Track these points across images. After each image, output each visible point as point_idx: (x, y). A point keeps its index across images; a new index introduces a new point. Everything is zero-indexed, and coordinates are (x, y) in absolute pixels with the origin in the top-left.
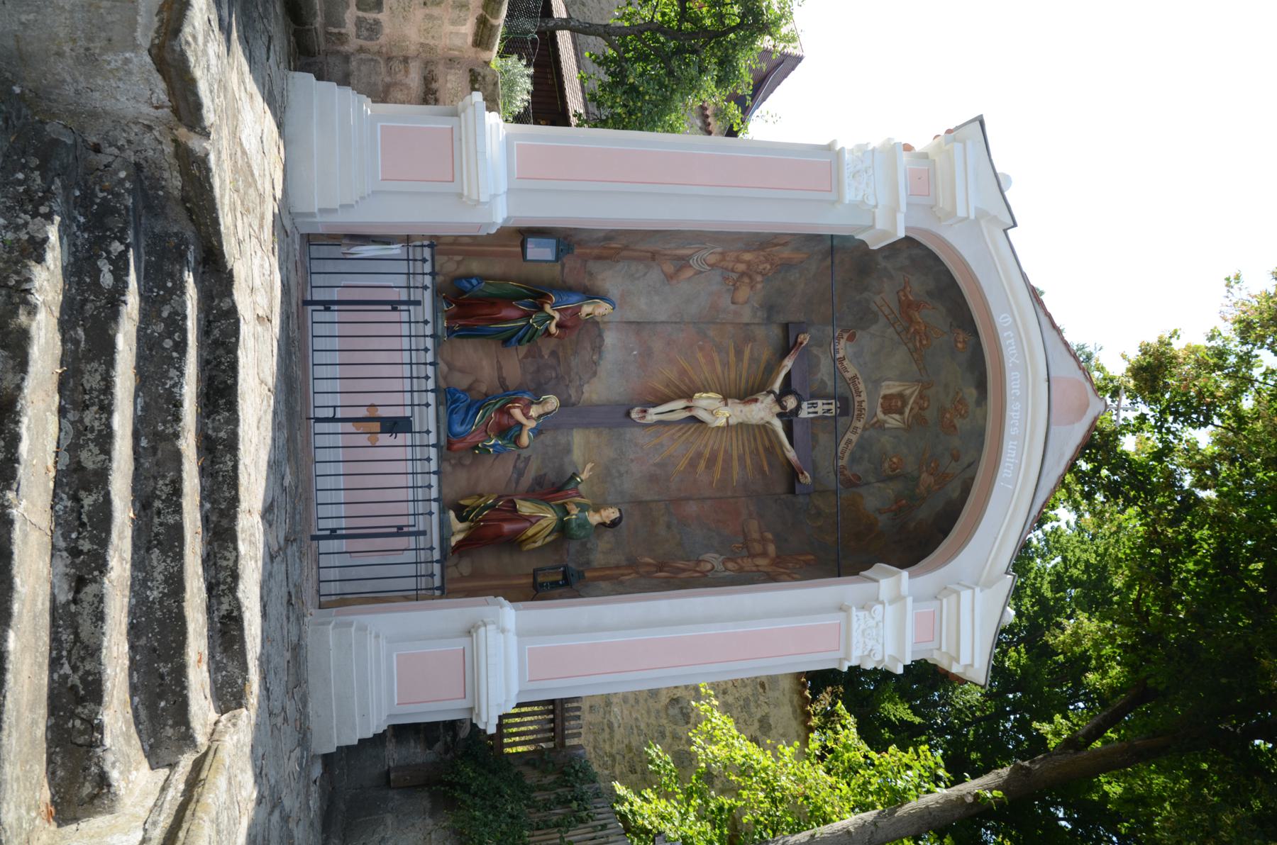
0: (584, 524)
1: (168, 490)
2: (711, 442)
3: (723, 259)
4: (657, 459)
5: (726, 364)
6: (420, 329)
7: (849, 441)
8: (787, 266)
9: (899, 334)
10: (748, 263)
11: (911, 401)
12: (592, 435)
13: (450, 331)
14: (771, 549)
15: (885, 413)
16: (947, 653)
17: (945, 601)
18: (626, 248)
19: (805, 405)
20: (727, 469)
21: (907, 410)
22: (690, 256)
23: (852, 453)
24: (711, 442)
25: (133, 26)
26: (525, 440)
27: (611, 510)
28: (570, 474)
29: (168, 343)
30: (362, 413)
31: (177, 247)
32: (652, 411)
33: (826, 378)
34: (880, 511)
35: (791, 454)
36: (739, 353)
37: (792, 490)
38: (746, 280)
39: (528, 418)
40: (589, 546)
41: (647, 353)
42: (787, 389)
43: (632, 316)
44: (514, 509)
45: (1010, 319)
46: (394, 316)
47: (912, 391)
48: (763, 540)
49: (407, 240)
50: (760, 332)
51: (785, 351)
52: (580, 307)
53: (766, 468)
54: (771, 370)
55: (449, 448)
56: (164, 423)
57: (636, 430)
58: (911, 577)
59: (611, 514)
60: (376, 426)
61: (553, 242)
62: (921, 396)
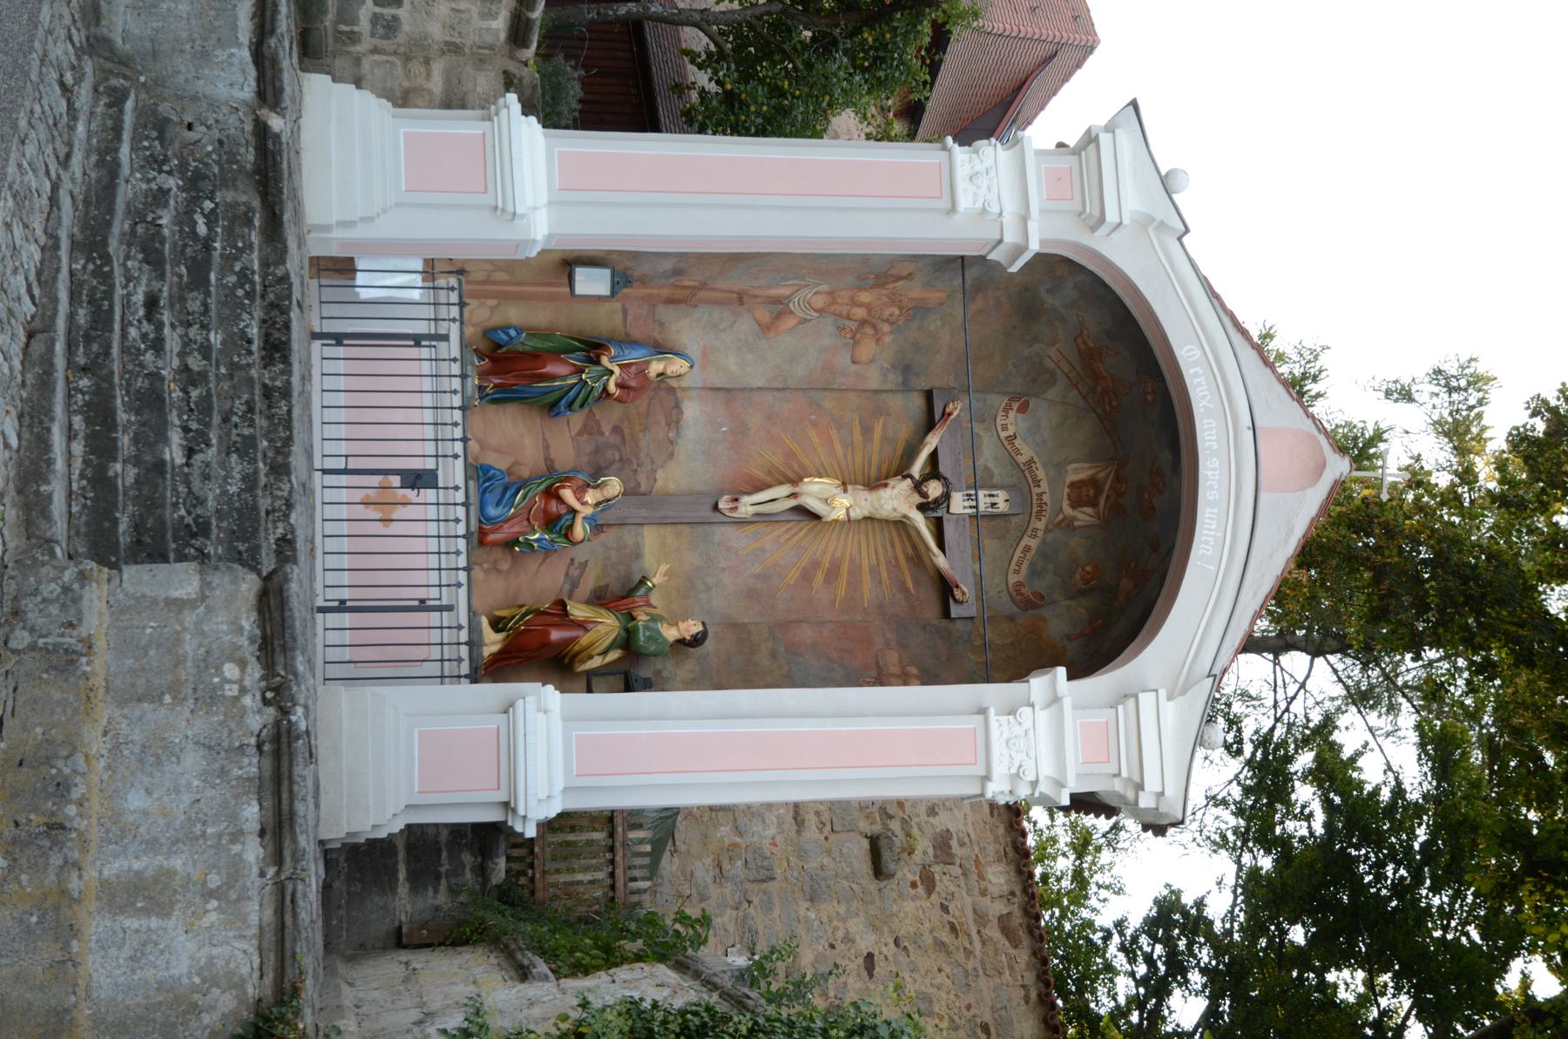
0: (656, 637)
2: (831, 548)
3: (834, 302)
4: (758, 569)
5: (849, 445)
6: (444, 368)
7: (1027, 549)
8: (920, 310)
9: (1084, 398)
10: (868, 307)
16: (1129, 780)
17: (1120, 708)
18: (703, 286)
21: (1102, 501)
22: (789, 298)
23: (1032, 564)
24: (831, 548)
25: (234, 28)
26: (579, 531)
27: (691, 622)
28: (637, 578)
32: (747, 499)
33: (991, 465)
34: (1069, 638)
35: (941, 561)
36: (867, 431)
38: (869, 331)
39: (584, 504)
40: (665, 674)
41: (740, 431)
42: (933, 470)
43: (720, 382)
44: (566, 613)
45: (1198, 352)
47: (1105, 474)
50: (896, 402)
51: (930, 425)
52: (648, 363)
53: (910, 584)
54: (910, 454)
55: (481, 543)
57: (729, 531)
58: (1070, 677)
59: (692, 628)
60: (396, 480)
61: (606, 273)
62: (1118, 479)
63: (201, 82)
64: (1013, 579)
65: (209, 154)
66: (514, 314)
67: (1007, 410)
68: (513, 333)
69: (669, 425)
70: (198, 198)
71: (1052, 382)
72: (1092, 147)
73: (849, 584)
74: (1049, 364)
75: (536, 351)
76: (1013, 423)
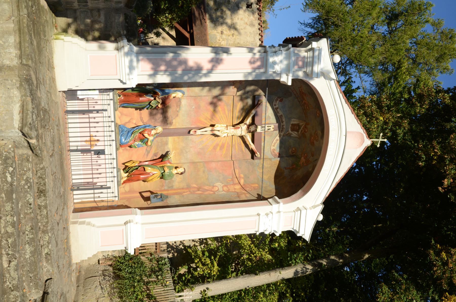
1: (30, 228)
4: (201, 146)
11: (302, 128)
15: (292, 131)
17: (296, 212)
21: (300, 131)
29: (26, 187)
31: (27, 158)
33: (270, 115)
34: (286, 168)
47: (302, 124)
56: (27, 210)
62: (305, 127)
64: (272, 148)
65: (10, 149)
67: (276, 100)
69: (177, 106)
70: (6, 167)
73: (226, 150)
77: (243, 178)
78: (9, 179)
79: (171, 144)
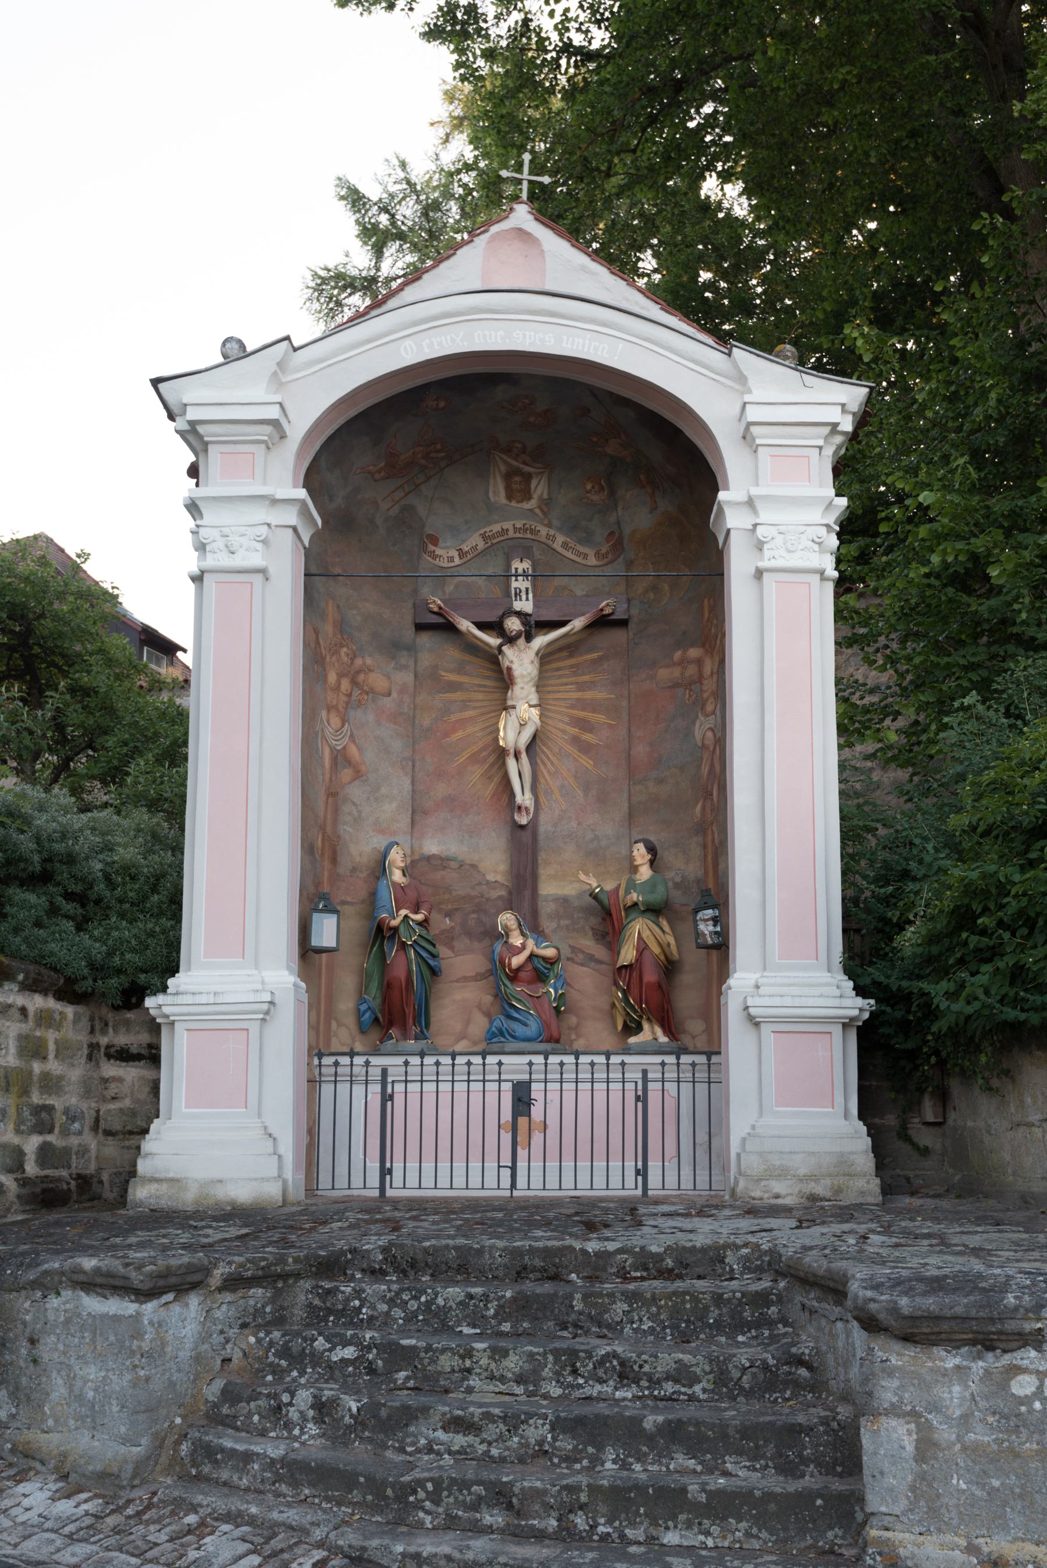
0: (651, 884)
2: (561, 725)
3: (335, 708)
5: (465, 705)
7: (565, 545)
8: (341, 626)
9: (428, 479)
10: (340, 675)
11: (514, 463)
12: (544, 872)
13: (420, 1036)
14: (694, 653)
15: (530, 498)
16: (826, 438)
17: (758, 441)
18: (323, 828)
19: (518, 606)
20: (593, 706)
21: (527, 469)
22: (332, 749)
23: (580, 541)
24: (561, 725)
26: (550, 953)
27: (635, 853)
28: (590, 900)
30: (507, 1138)
32: (519, 799)
34: (653, 509)
35: (578, 624)
37: (623, 623)
38: (361, 677)
39: (524, 947)
40: (678, 879)
41: (451, 803)
42: (495, 627)
43: (405, 820)
44: (629, 967)
45: (408, 342)
46: (399, 1099)
48: (683, 662)
49: (314, 1083)
50: (426, 660)
51: (449, 628)
53: (595, 655)
54: (473, 648)
57: (543, 818)
59: (640, 854)
61: (316, 916)
62: (508, 451)
63: (181, 1354)
64: (592, 561)
65: (259, 1341)
66: (346, 1005)
67: (435, 557)
68: (363, 1008)
69: (445, 867)
70: (313, 1354)
71: (409, 509)
72: (201, 429)
73: (594, 711)
74: (395, 511)
75: (381, 984)
76: (447, 554)
77: (685, 651)
78: (349, 1352)
79: (563, 882)
